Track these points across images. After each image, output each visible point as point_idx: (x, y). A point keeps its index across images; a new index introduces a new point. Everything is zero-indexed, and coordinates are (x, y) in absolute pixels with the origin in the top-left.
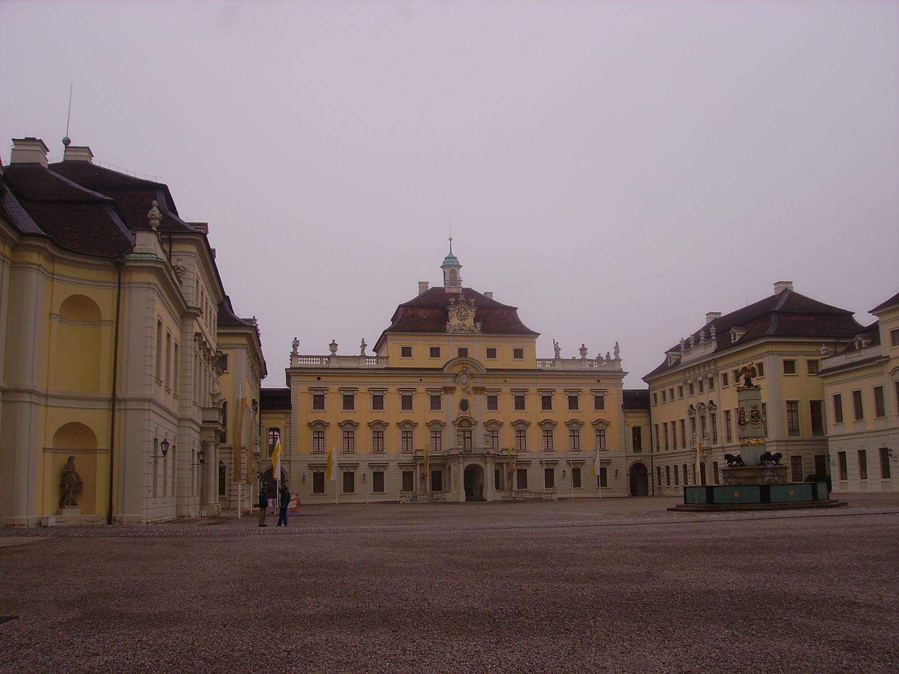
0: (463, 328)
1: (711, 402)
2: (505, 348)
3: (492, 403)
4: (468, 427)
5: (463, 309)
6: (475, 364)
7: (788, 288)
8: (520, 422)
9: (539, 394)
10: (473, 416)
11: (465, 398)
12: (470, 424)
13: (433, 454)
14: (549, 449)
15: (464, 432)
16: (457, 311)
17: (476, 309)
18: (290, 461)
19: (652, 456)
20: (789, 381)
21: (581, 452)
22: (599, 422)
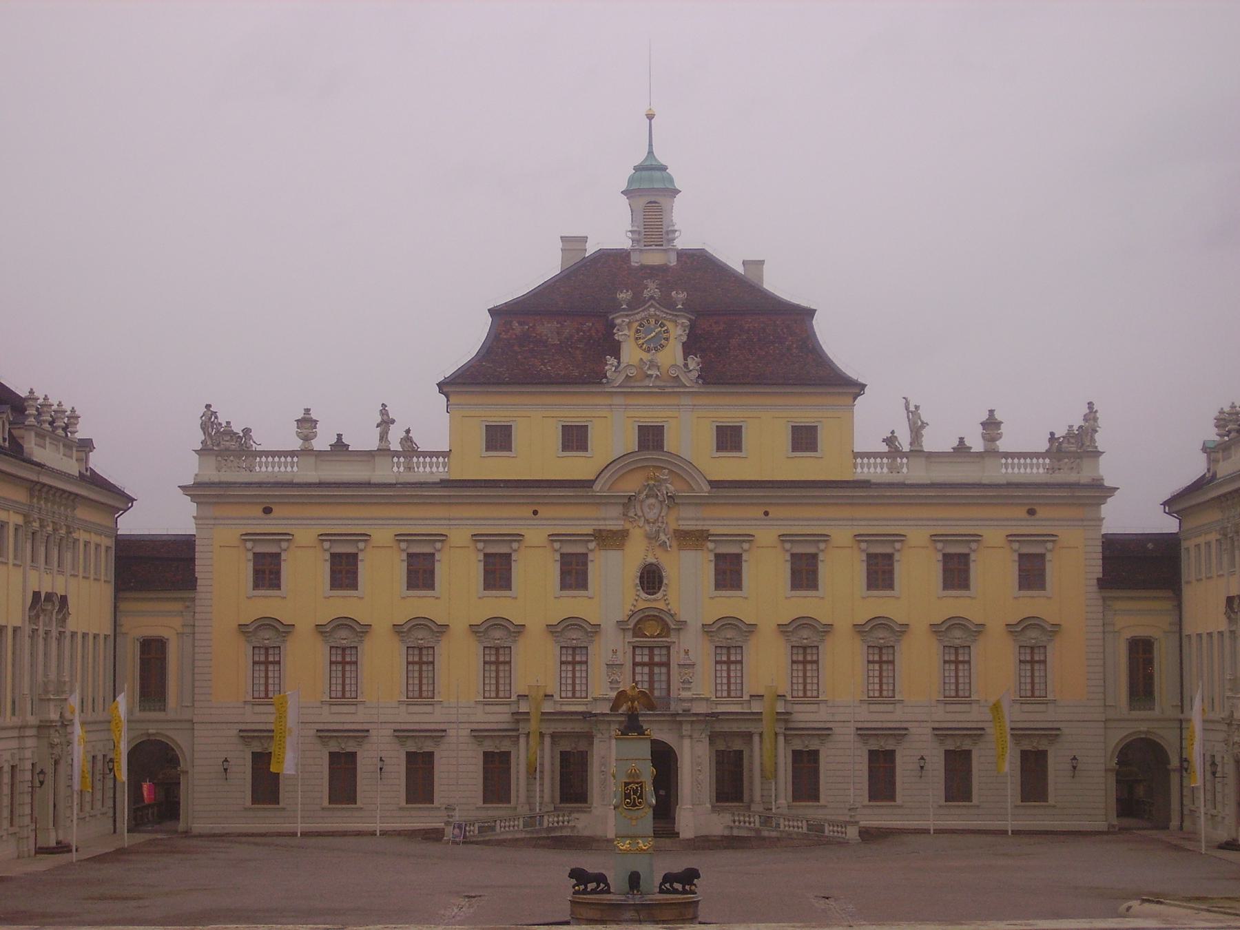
0: (649, 372)
4: (658, 636)
5: (653, 321)
6: (680, 468)
8: (803, 623)
9: (553, 547)
10: (674, 607)
11: (654, 561)
12: (666, 630)
14: (883, 694)
15: (651, 649)
16: (635, 325)
17: (690, 320)
18: (191, 721)
19: (1181, 721)
21: (975, 707)
22: (1030, 623)
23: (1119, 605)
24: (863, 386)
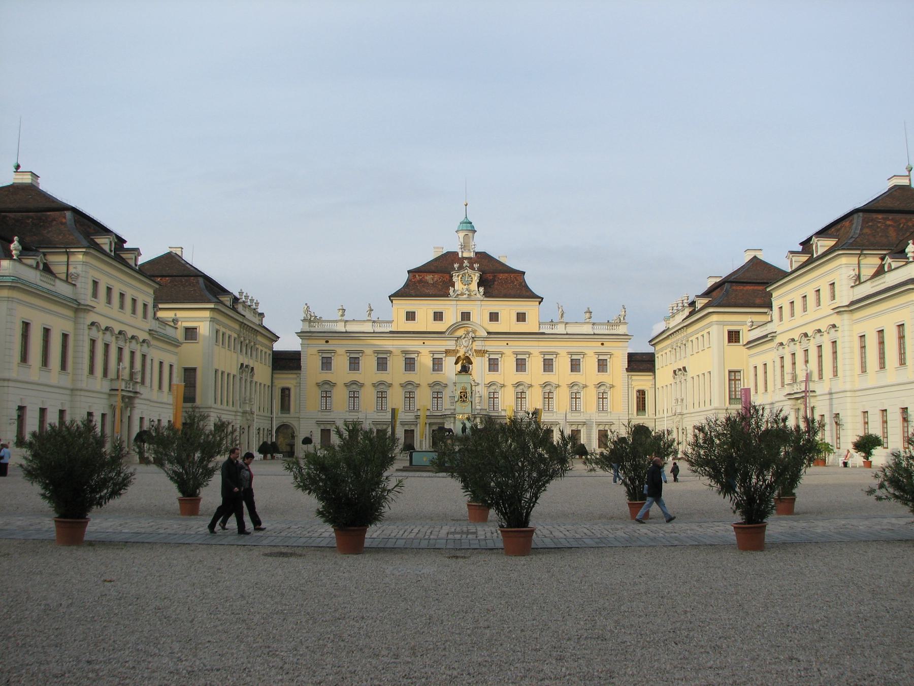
1: (684, 368)
2: (508, 309)
3: (493, 365)
7: (758, 257)
13: (434, 414)
20: (735, 348)
23: (634, 378)
24: (542, 299)
